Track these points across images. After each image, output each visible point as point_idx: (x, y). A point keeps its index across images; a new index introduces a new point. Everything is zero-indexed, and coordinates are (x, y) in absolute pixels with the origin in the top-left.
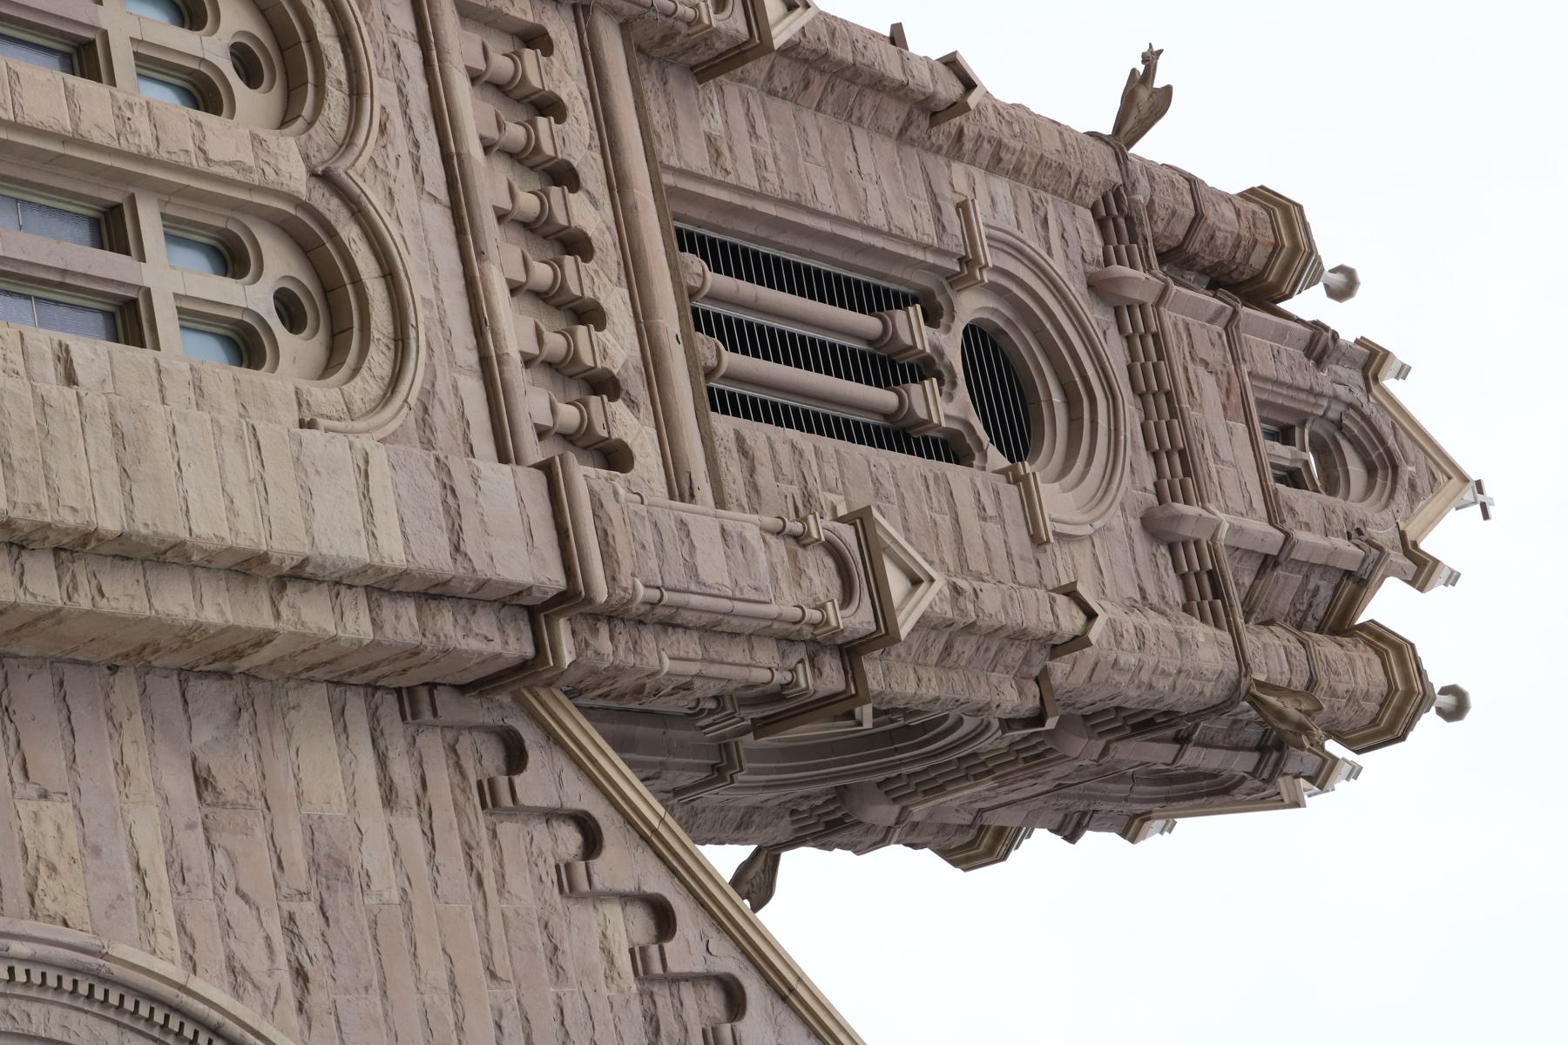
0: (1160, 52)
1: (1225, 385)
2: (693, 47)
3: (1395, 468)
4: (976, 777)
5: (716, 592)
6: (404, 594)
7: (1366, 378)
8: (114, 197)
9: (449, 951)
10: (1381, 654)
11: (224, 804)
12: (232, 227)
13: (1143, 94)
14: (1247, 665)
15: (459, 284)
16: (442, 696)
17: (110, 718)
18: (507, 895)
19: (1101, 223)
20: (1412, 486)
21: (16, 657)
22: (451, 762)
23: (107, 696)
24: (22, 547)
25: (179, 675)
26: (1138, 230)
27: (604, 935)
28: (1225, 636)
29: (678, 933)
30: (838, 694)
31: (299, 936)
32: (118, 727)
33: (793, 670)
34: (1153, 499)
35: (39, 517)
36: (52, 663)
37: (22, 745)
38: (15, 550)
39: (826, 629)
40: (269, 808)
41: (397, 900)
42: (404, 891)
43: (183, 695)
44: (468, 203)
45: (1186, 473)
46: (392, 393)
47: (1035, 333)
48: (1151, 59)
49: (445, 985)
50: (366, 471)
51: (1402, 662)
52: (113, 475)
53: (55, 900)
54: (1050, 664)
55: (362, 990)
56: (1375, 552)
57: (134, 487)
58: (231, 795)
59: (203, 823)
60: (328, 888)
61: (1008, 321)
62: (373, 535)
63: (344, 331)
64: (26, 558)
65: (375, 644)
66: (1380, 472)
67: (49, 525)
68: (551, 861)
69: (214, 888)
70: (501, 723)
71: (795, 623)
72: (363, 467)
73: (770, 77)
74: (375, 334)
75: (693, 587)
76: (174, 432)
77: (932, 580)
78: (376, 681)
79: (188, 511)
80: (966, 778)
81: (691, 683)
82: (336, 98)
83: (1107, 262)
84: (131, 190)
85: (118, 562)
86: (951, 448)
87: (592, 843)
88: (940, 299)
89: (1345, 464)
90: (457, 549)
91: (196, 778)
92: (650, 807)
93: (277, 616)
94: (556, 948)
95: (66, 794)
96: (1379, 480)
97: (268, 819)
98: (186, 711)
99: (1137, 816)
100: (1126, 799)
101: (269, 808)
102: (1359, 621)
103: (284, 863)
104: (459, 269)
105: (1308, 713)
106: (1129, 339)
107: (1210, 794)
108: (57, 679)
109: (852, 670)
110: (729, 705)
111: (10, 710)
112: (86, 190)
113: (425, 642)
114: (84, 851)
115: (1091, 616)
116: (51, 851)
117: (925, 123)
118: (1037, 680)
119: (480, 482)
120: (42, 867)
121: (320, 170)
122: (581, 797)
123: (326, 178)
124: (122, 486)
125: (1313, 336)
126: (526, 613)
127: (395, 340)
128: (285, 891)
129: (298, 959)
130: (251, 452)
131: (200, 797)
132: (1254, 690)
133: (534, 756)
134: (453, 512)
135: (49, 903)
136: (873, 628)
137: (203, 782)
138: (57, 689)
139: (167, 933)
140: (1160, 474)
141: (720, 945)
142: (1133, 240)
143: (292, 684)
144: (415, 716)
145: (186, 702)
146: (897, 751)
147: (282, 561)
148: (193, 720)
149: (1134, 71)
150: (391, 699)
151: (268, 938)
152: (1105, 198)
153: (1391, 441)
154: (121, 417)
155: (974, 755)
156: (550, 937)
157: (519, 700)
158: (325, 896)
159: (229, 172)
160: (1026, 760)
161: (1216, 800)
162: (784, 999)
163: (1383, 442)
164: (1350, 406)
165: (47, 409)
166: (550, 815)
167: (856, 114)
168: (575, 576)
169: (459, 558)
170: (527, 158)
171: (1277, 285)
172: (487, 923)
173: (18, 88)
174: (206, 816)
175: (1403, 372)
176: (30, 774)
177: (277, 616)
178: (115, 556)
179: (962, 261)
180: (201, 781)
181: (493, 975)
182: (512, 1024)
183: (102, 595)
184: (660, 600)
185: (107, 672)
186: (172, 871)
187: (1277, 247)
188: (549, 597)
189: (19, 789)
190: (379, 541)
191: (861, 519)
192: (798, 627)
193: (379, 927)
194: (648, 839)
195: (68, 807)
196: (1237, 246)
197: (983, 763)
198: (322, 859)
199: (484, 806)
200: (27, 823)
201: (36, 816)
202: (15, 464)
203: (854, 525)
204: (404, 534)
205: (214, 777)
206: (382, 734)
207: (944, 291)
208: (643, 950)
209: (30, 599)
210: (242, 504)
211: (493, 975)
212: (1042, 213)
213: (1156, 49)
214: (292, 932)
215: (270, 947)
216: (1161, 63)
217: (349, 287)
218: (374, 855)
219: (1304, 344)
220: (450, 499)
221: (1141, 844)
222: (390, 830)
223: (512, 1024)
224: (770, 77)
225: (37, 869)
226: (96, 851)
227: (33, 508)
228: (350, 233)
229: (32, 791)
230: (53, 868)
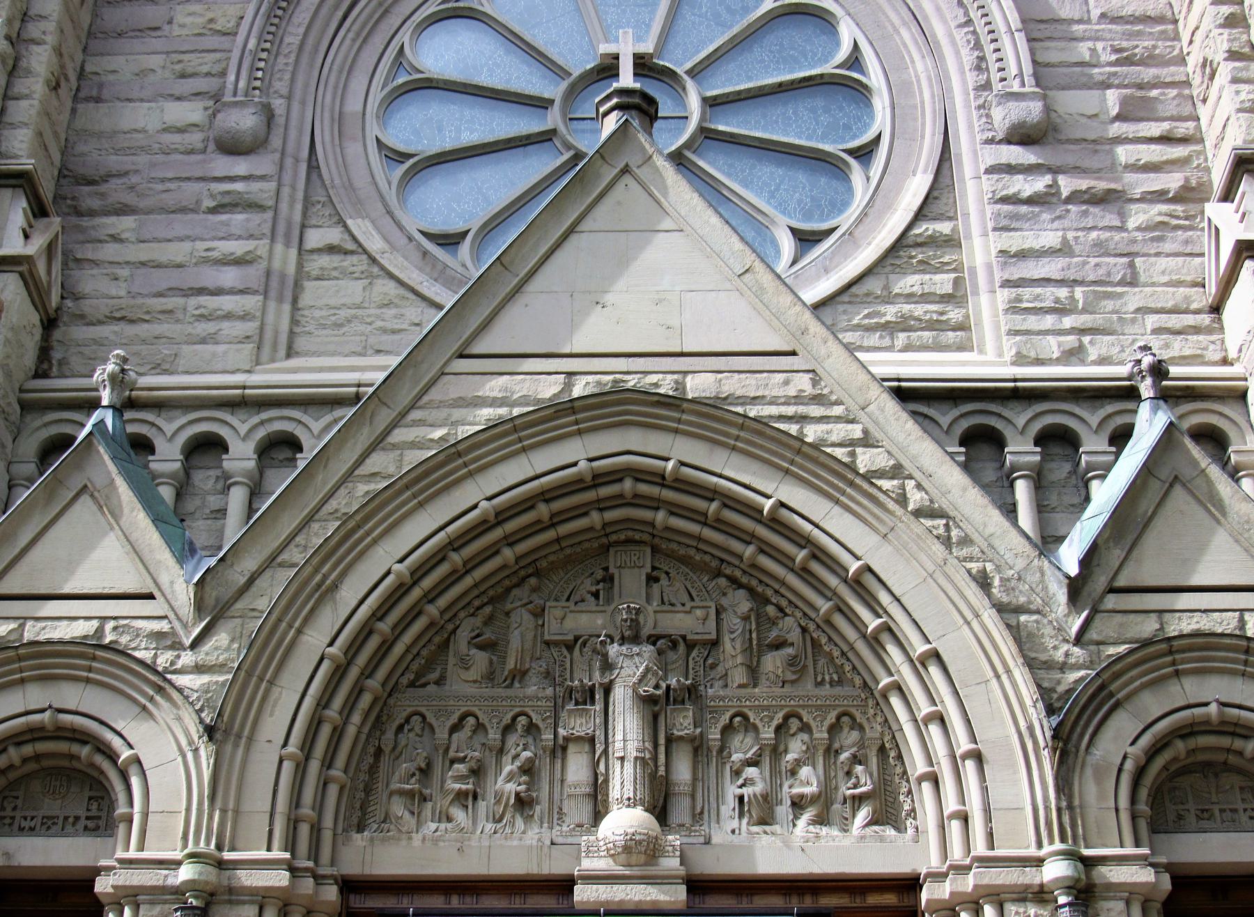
24: (25, 14)
38: (26, 18)
53: (229, 22)
64: (31, 13)
116: (200, 20)
120: (210, 26)
135: (230, 25)
189: (165, 33)
200: (184, 32)
201: (182, 26)
225: (210, 29)
229: (166, 27)
230: (211, 21)
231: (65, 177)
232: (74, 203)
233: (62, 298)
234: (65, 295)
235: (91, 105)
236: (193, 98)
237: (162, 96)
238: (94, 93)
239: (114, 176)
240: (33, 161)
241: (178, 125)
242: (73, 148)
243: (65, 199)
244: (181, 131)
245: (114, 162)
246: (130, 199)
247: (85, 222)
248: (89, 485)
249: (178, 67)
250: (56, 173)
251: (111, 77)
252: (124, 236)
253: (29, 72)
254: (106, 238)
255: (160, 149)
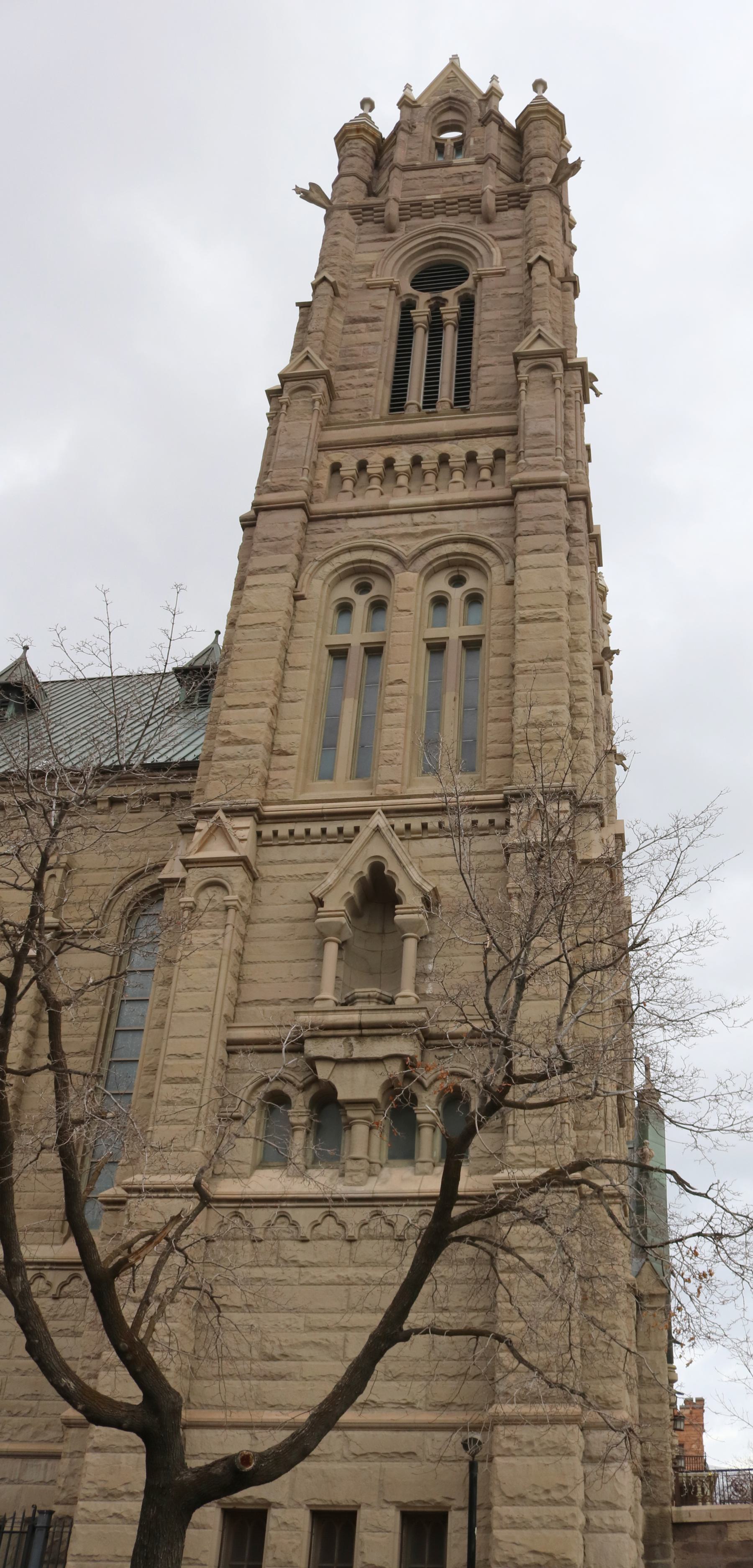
28: (535, 194)
48: (298, 190)
77: (539, 330)
86: (467, 303)
88: (404, 299)
96: (455, 106)
102: (514, 126)
106: (412, 216)
115: (540, 258)
163: (439, 103)
171: (377, 139)
175: (408, 87)
207: (401, 298)
216: (300, 186)
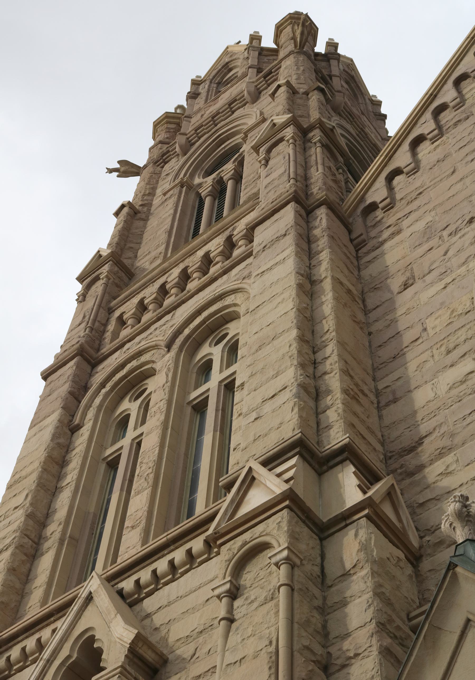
0: (107, 168)
1: (208, 108)
2: (119, 278)
3: (227, 63)
4: (366, 134)
5: (288, 167)
6: (309, 249)
7: (202, 83)
8: (189, 410)
9: (449, 188)
10: (281, 32)
11: (413, 276)
12: (195, 370)
13: (122, 169)
14: (290, 52)
15: (201, 294)
16: (354, 236)
17: (389, 325)
18: (423, 184)
19: (166, 163)
20: (231, 56)
21: (373, 365)
22: (379, 224)
23: (381, 330)
25: (367, 314)
26: (165, 151)
27: (429, 153)
29: (421, 133)
30: (321, 130)
31: (456, 229)
32: (392, 321)
33: (315, 143)
34: (247, 105)
35: (296, 355)
36: (373, 353)
37: (407, 345)
39: (296, 137)
40: (411, 263)
41: (434, 212)
42: (430, 211)
43: (375, 309)
44: (173, 304)
45: (236, 100)
46: (239, 289)
47: (204, 162)
48: (110, 171)
49: (462, 183)
50: (261, 273)
51: (282, 24)
52: (275, 342)
53: (465, 305)
54: (301, 93)
55: (472, 202)
56: (250, 48)
57: (279, 333)
58: (408, 274)
59: (422, 278)
60: (435, 231)
61: (202, 170)
62: (284, 259)
63: (224, 318)
65: (330, 247)
66: (230, 67)
67: (298, 351)
68: (407, 179)
69: (446, 263)
70: (360, 216)
71: (296, 146)
72: (260, 275)
73: (130, 258)
74: (221, 306)
75: (287, 172)
76: (256, 333)
78: (354, 257)
79: (285, 313)
80: (368, 137)
81: (327, 167)
82: (143, 359)
83: (178, 155)
84: (185, 404)
85: (315, 333)
87: (398, 172)
89: (230, 77)
90: (285, 235)
91: (405, 289)
92: (378, 161)
93: (326, 277)
94: (438, 161)
95: (422, 323)
96: (233, 65)
97: (415, 261)
98: (381, 305)
99: (372, 103)
100: (366, 104)
101: (411, 263)
103: (430, 248)
104: (196, 296)
105: (298, 25)
107: (356, 82)
108: (378, 349)
109: (311, 128)
110: (339, 165)
111: (394, 356)
112: (188, 418)
113: (325, 235)
114: (444, 307)
117: (139, 215)
118: (308, 95)
119: (260, 243)
120: (454, 315)
121: (166, 350)
122: (381, 180)
123: (169, 347)
124: (279, 337)
125: (190, 98)
126: (310, 215)
127: (222, 299)
128: (441, 242)
129: (465, 225)
130: (260, 307)
131: (412, 284)
132: (298, 48)
133: (369, 200)
134: (272, 243)
136: (292, 126)
137: (406, 286)
138: (382, 347)
139: (468, 266)
140: (239, 108)
141: (422, 120)
142: (168, 152)
143: (362, 281)
144: (364, 241)
145: (377, 307)
146: (364, 158)
147: (299, 279)
148: (383, 301)
149: (118, 176)
150: (360, 252)
151: (460, 238)
152: (158, 166)
153: (220, 68)
154: (253, 350)
155: (357, 135)
156: (435, 165)
157: (350, 215)
158: (439, 231)
159: (170, 375)
160: (353, 119)
161: (357, 80)
162: (435, 96)
163: (220, 70)
164: (211, 82)
165: (253, 373)
166: (390, 188)
167: (140, 233)
168: (288, 200)
169: (288, 233)
170: (160, 302)
172: (434, 184)
173: (147, 450)
174: (419, 279)
176: (417, 337)
177: (326, 277)
178: (313, 335)
179: (182, 187)
180: (406, 287)
181: (453, 172)
182: (470, 158)
183: (328, 330)
184: (293, 178)
185: (372, 335)
186: (444, 277)
187: (167, 123)
188: (298, 206)
189: (425, 338)
190: (286, 256)
191: (256, 148)
192: (297, 145)
193: (446, 210)
194: (390, 157)
195: (427, 321)
196: (169, 132)
197: (360, 132)
198: (425, 239)
199: (392, 208)
200: (437, 330)
202: (275, 372)
203: (259, 149)
204: (282, 252)
205: (402, 283)
206: (374, 246)
208: (431, 140)
209: (335, 351)
210: (279, 300)
211: (453, 172)
212: (165, 177)
213: (107, 170)
214: (456, 232)
215: (463, 235)
216: (111, 167)
217: (207, 323)
218: (420, 226)
219: (193, 100)
220: (267, 247)
221: (381, 100)
222: (409, 227)
223: (470, 158)
224: (130, 258)
225: (455, 316)
226: (442, 304)
227: (292, 358)
228: (187, 331)
229: (424, 334)
230: (453, 311)
231: (390, 458)
232: (404, 469)
233: (421, 538)
234: (422, 535)
235: (392, 406)
236: (462, 359)
237: (438, 372)
238: (391, 398)
239: (426, 436)
240: (348, 435)
241: (459, 379)
242: (389, 438)
243: (396, 470)
244: (462, 382)
245: (424, 429)
246: (446, 442)
247: (417, 477)
248: (471, 617)
249: (443, 348)
250: (382, 457)
251: (399, 383)
252: (451, 469)
253: (329, 392)
254: (437, 478)
255: (453, 401)
